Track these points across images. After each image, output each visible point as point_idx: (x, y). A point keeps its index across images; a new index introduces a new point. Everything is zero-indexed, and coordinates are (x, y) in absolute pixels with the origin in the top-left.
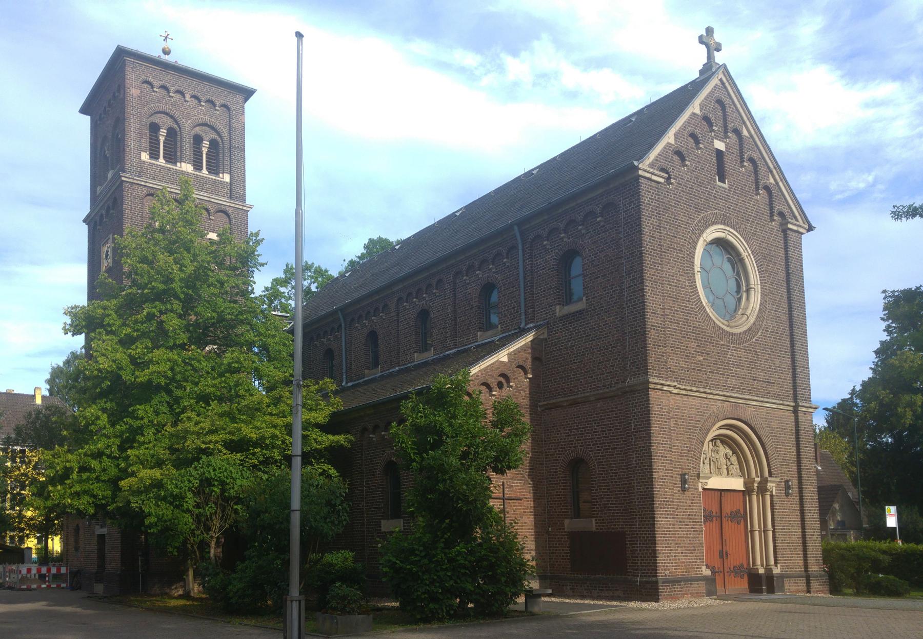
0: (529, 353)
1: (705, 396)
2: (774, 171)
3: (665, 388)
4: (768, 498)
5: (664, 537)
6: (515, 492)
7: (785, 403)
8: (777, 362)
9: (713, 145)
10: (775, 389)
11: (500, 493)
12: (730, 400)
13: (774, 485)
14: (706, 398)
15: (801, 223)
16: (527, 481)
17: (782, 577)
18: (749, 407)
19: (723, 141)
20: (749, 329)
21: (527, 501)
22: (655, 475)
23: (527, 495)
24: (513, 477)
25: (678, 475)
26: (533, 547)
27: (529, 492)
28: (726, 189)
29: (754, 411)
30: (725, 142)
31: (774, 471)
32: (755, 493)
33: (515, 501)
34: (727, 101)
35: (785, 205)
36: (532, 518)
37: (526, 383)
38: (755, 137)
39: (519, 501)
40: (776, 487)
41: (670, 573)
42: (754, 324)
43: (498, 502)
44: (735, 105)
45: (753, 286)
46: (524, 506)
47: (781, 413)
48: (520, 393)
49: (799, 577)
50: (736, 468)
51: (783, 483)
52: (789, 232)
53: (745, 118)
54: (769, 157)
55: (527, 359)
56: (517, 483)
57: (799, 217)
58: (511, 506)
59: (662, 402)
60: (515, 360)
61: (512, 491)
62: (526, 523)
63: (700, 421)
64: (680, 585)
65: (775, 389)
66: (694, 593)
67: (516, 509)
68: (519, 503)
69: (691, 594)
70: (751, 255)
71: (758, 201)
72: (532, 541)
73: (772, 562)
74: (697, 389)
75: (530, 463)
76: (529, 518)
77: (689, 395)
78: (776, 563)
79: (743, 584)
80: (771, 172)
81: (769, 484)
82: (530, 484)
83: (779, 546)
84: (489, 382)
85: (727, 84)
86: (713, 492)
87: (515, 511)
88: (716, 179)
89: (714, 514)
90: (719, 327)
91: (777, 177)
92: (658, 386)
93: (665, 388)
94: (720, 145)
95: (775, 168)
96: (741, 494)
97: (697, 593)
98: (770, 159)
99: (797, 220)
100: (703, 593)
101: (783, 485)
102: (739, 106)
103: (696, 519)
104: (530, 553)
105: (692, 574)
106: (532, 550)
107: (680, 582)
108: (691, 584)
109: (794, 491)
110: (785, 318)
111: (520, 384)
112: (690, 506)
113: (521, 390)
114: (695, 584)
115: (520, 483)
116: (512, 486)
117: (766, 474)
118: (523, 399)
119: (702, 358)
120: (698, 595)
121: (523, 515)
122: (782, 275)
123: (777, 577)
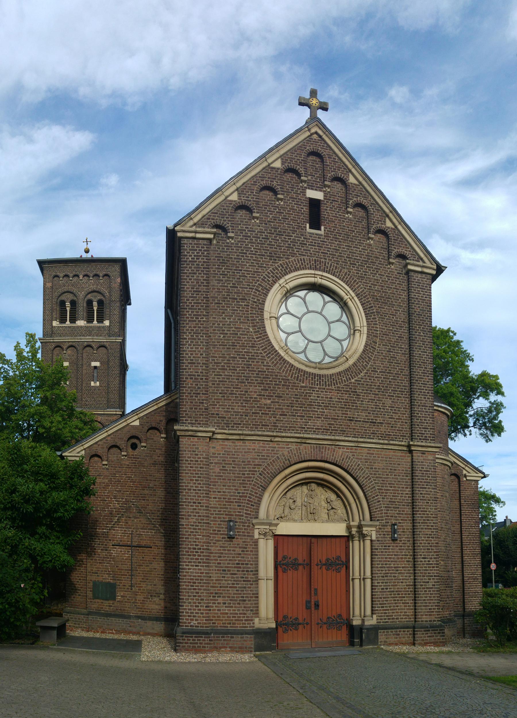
0: (163, 416)
1: (268, 439)
2: (391, 215)
3: (200, 434)
4: (368, 543)
5: (192, 586)
6: (146, 540)
7: (392, 442)
8: (389, 402)
9: (305, 195)
10: (383, 429)
11: (128, 541)
12: (307, 442)
13: (374, 529)
14: (271, 441)
15: (428, 264)
16: (159, 530)
17: (375, 629)
18: (339, 448)
19: (321, 191)
20: (347, 370)
21: (158, 549)
22: (183, 522)
23: (159, 543)
24: (144, 526)
25: (225, 521)
26: (162, 591)
27: (161, 541)
28: (322, 235)
29: (346, 452)
30: (324, 191)
31: (376, 515)
32: (357, 539)
33: (145, 549)
34: (325, 153)
35: (408, 248)
36: (162, 564)
37: (163, 442)
38: (364, 183)
39: (149, 549)
40: (377, 532)
41: (198, 623)
42: (355, 364)
43: (126, 549)
44: (337, 155)
45: (359, 328)
46: (155, 553)
47: (392, 453)
48: (155, 451)
49: (401, 628)
50: (341, 511)
51: (389, 527)
52: (412, 274)
53: (350, 166)
54: (383, 202)
55: (161, 421)
56: (147, 532)
57: (425, 259)
58: (140, 552)
59: (198, 448)
60: (148, 423)
61: (141, 540)
62: (155, 569)
63: (261, 465)
64: (209, 637)
65: (383, 429)
66: (235, 648)
67: (145, 555)
68: (148, 550)
69: (230, 647)
70: (356, 298)
71: (371, 245)
72: (162, 585)
73: (369, 612)
74: (292, 435)
75: (162, 514)
76: (159, 564)
77: (245, 440)
78: (373, 612)
79: (343, 635)
80: (388, 216)
81: (364, 529)
82: (162, 533)
83: (378, 594)
84: (118, 445)
85: (324, 137)
86: (300, 538)
87: (143, 558)
88: (306, 227)
89: (300, 561)
90: (298, 369)
91: (394, 220)
92: (190, 433)
93: (200, 434)
94: (312, 194)
95: (391, 212)
96: (343, 540)
97: (240, 648)
98: (384, 203)
99: (424, 262)
100: (251, 648)
101: (389, 529)
102: (341, 155)
103: (250, 568)
104: (159, 596)
105: (239, 626)
106: (161, 594)
107: (210, 634)
108: (233, 637)
109: (405, 536)
110: (402, 358)
111: (155, 444)
112: (240, 554)
113: (156, 449)
114: (238, 638)
115: (151, 532)
116: (142, 535)
117: (361, 518)
118: (158, 457)
119: (269, 402)
120: (242, 650)
121: (153, 561)
122: (402, 316)
123: (367, 629)
